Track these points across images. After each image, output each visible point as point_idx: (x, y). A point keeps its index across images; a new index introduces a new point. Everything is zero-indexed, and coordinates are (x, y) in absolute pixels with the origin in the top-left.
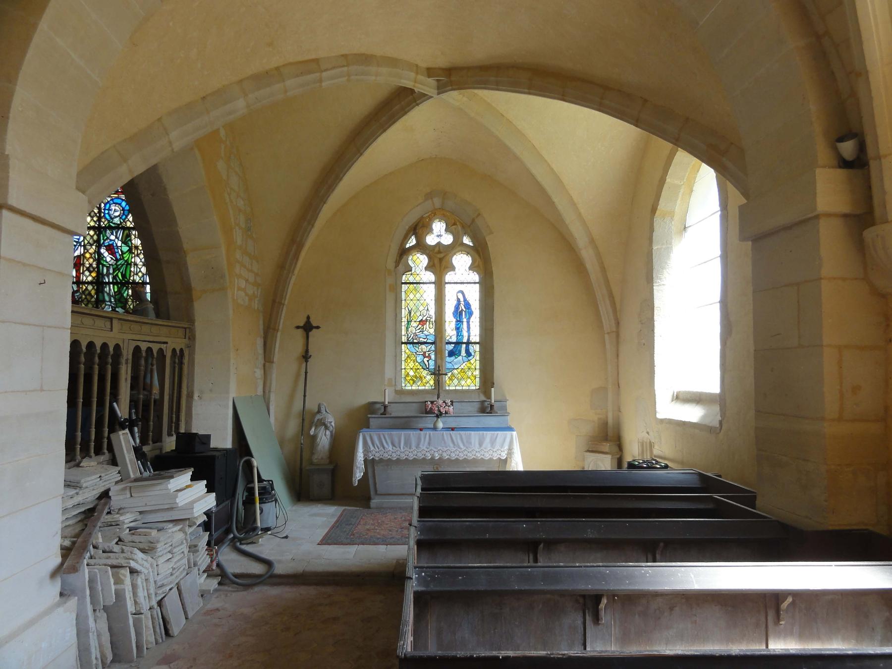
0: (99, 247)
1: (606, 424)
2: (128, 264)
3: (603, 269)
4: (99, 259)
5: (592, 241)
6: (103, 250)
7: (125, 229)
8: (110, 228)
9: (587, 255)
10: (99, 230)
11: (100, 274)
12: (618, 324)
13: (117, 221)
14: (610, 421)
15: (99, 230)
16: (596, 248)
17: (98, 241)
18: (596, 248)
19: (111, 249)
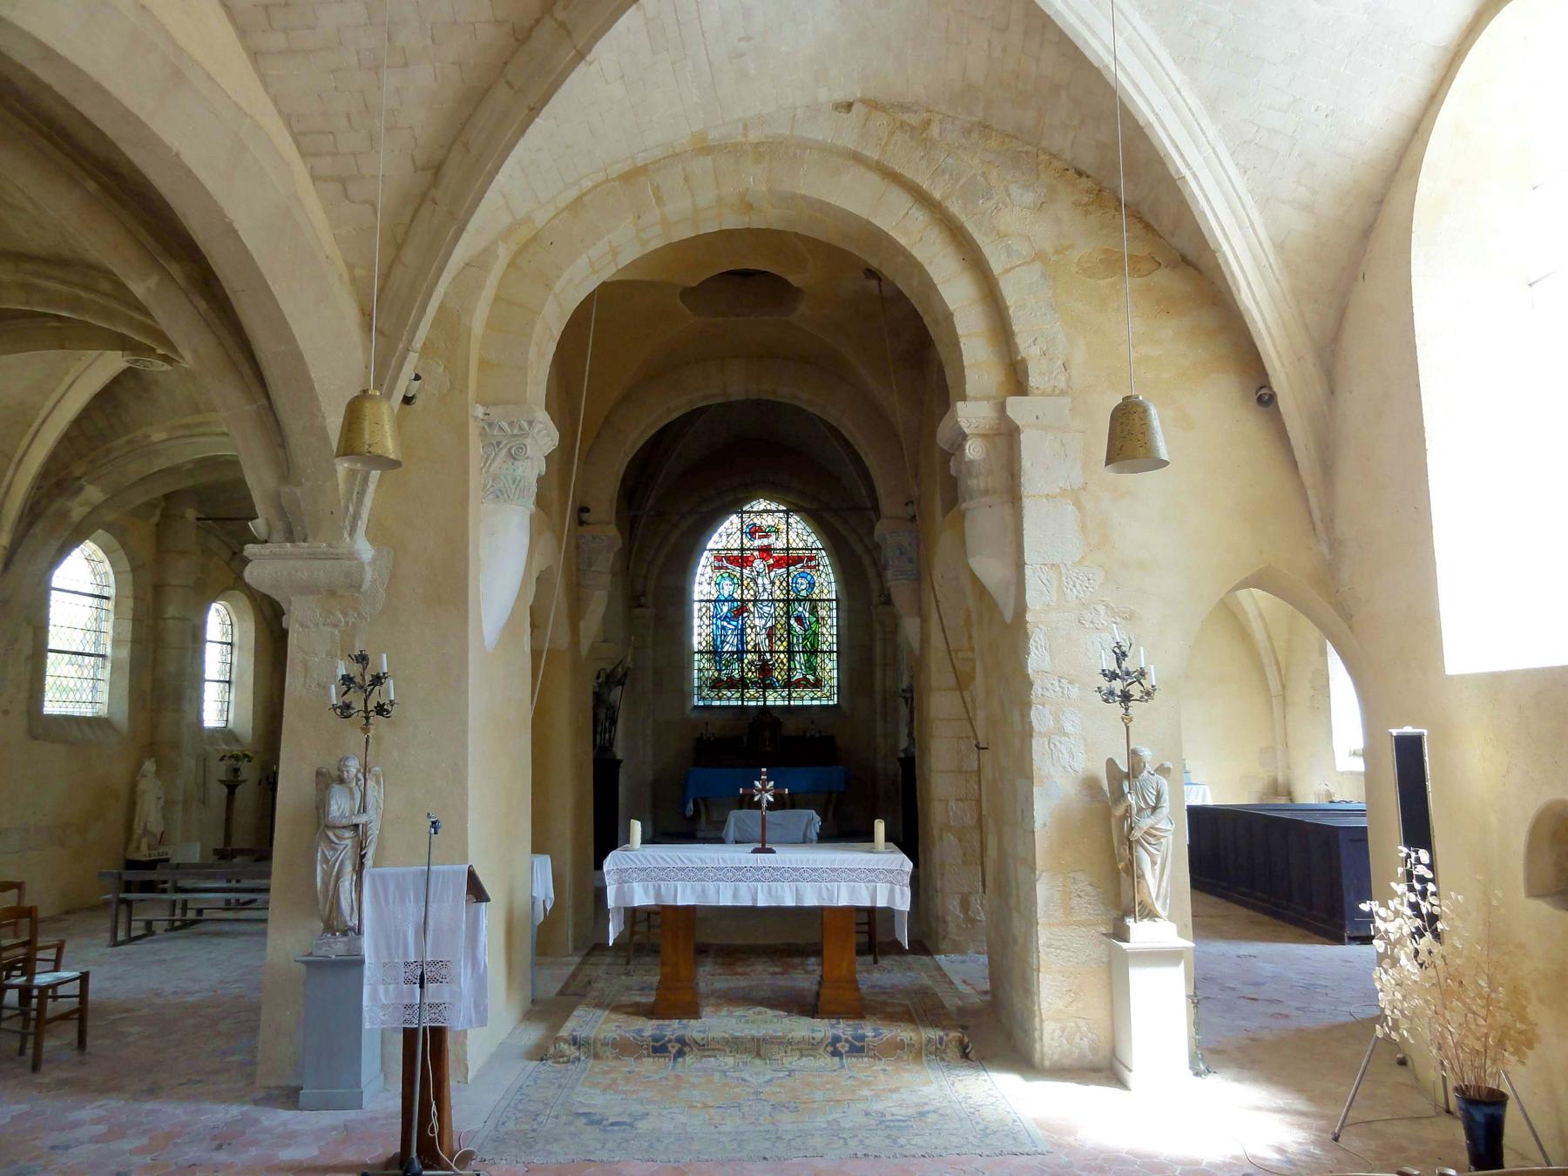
0: (789, 618)
1: (1276, 780)
2: (816, 634)
3: (1270, 639)
4: (789, 628)
5: (1261, 615)
6: (792, 621)
7: (811, 600)
8: (799, 601)
9: (1257, 628)
10: (788, 602)
11: (790, 644)
12: (1284, 687)
13: (804, 593)
14: (1281, 779)
15: (788, 602)
16: (1263, 619)
17: (787, 613)
18: (1263, 619)
19: (799, 619)
